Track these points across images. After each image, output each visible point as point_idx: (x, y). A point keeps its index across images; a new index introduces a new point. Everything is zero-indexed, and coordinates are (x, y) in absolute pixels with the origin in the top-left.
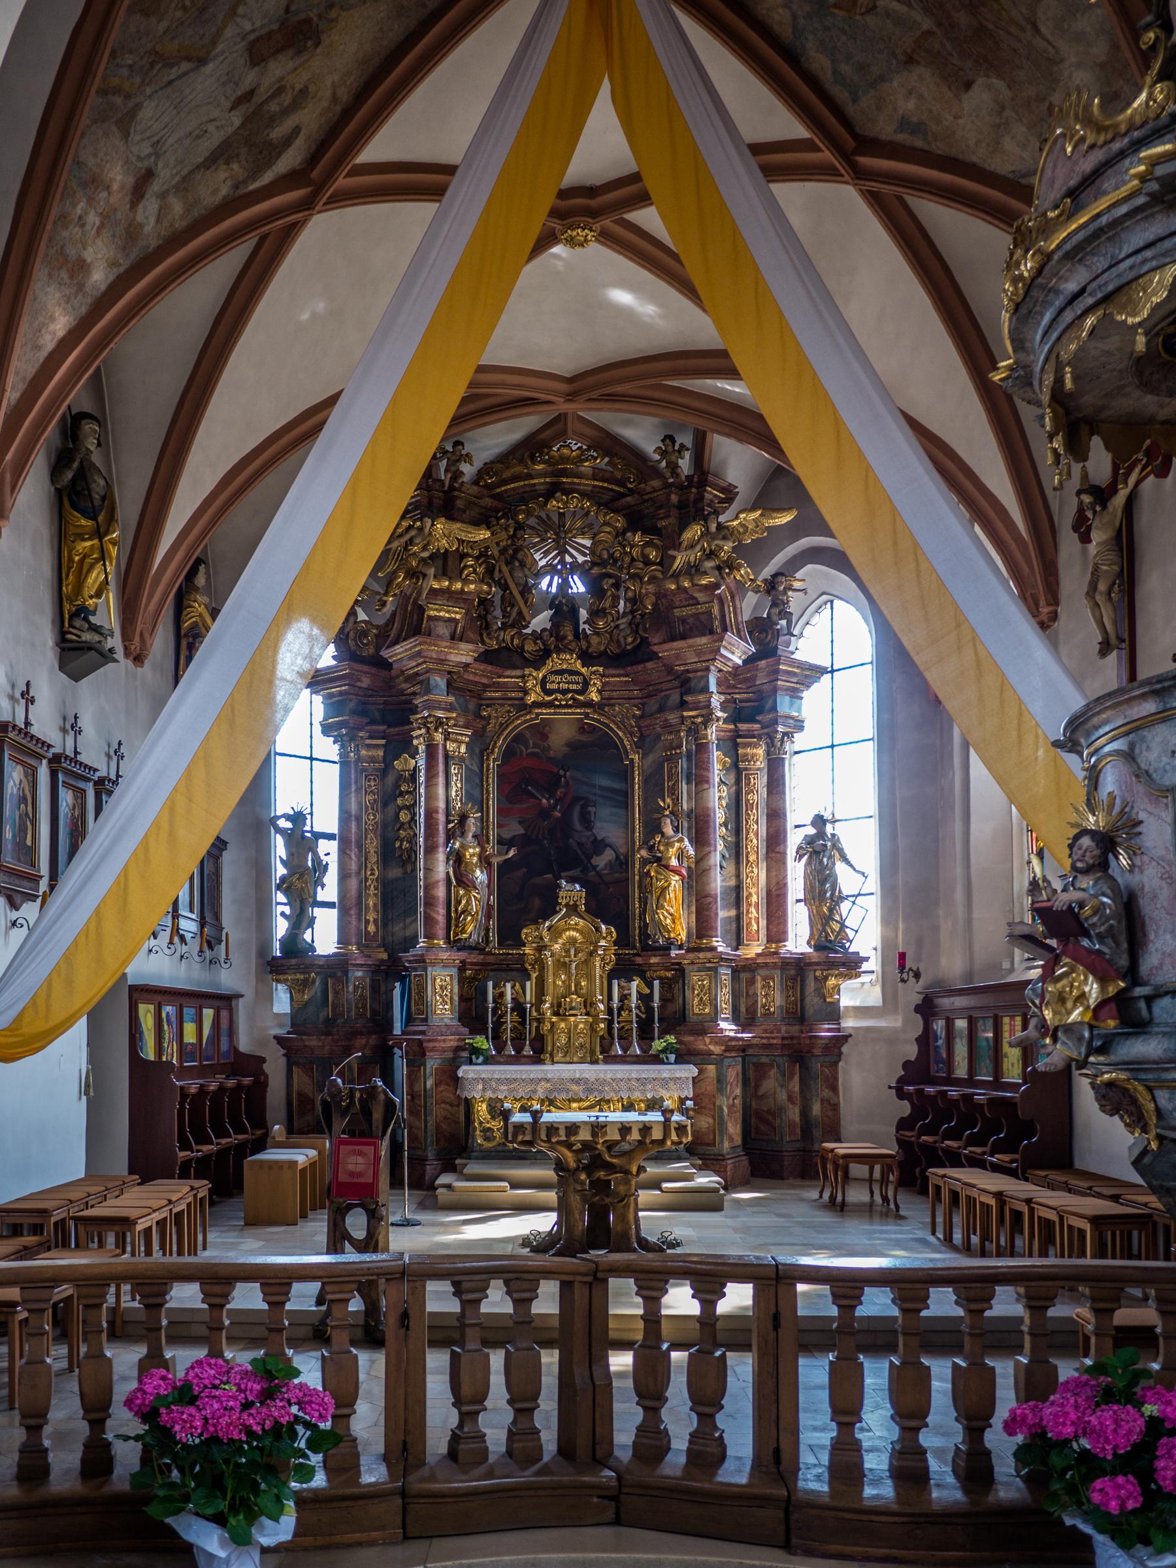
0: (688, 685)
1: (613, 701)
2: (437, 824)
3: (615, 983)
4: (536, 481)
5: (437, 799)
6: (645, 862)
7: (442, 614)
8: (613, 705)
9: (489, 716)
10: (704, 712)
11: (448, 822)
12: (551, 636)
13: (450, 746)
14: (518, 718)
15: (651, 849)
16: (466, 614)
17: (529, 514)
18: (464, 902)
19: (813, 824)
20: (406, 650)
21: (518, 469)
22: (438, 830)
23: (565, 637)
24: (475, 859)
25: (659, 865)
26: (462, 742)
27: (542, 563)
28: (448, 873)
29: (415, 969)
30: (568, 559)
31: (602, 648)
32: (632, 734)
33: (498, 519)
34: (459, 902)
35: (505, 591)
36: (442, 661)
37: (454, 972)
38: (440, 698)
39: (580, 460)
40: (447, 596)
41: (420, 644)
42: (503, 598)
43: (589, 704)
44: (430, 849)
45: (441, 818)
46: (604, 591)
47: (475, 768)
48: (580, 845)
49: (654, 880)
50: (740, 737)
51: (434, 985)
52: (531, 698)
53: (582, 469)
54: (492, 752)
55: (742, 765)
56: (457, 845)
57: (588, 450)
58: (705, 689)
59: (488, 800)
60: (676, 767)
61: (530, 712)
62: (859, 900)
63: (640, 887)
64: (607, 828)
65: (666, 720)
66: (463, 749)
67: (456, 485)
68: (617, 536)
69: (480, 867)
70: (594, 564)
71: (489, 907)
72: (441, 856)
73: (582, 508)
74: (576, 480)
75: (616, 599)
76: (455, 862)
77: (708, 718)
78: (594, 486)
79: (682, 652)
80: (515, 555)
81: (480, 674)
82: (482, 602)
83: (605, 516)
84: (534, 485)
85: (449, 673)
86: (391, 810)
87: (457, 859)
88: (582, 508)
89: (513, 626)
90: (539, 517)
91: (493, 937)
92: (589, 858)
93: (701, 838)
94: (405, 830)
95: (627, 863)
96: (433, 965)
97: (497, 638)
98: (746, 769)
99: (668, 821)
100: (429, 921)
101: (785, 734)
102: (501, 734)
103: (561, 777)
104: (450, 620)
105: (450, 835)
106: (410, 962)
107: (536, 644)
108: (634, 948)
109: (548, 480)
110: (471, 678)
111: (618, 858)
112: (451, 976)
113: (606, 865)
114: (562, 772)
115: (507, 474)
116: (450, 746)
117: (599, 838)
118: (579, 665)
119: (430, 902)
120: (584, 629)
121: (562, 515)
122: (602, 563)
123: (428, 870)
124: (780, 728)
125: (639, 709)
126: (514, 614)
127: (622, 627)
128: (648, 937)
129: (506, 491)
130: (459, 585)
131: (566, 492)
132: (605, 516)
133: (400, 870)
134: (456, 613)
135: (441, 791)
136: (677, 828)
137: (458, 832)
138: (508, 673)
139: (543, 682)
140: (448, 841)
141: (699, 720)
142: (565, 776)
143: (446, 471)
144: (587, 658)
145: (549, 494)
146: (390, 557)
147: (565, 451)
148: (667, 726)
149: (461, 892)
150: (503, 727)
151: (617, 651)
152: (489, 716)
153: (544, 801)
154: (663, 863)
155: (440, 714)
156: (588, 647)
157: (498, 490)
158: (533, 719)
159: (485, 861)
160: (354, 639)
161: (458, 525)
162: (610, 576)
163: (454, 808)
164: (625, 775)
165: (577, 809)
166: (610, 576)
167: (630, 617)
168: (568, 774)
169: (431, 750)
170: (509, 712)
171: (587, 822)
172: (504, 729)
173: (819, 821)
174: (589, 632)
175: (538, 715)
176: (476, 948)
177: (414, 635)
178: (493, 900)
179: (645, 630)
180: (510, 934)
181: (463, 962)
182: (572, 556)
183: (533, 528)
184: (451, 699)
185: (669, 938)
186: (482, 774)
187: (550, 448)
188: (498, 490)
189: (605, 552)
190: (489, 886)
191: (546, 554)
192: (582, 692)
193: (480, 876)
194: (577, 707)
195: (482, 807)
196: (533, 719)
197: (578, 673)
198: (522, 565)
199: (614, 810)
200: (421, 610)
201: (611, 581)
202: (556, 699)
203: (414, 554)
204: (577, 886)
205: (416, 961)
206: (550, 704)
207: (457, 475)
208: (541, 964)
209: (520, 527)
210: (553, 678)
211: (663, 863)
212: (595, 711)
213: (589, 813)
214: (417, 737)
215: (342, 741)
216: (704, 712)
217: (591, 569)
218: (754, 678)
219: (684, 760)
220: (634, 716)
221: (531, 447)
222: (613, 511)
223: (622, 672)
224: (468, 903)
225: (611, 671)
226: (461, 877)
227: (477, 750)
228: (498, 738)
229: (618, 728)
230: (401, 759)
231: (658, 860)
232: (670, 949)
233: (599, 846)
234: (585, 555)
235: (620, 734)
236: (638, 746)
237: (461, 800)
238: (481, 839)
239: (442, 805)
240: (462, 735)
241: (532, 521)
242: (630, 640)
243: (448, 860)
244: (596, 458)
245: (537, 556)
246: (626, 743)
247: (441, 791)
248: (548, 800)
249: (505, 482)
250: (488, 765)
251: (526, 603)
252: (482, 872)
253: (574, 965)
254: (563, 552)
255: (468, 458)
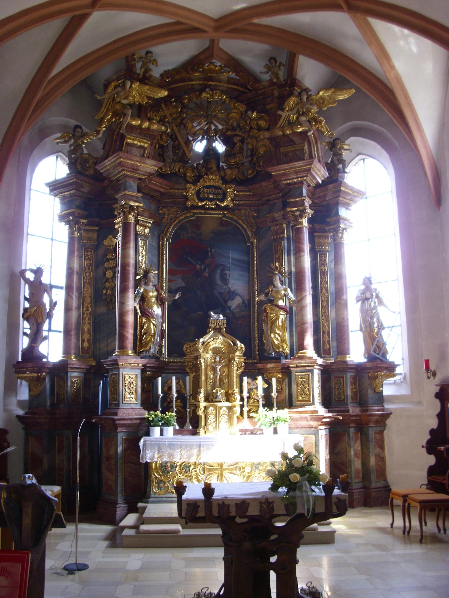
0: (292, 190)
1: (241, 207)
2: (129, 274)
3: (245, 379)
4: (194, 83)
5: (129, 257)
6: (261, 303)
7: (136, 142)
8: (240, 210)
9: (164, 213)
10: (301, 208)
11: (136, 274)
12: (203, 168)
13: (139, 229)
14: (182, 215)
15: (267, 295)
16: (151, 144)
17: (190, 100)
18: (146, 326)
19: (364, 284)
20: (112, 163)
21: (184, 74)
22: (129, 277)
23: (211, 168)
24: (154, 300)
25: (272, 305)
26: (145, 227)
27: (198, 128)
28: (135, 308)
29: (112, 370)
30: (213, 127)
31: (234, 177)
32: (251, 227)
33: (171, 103)
34: (142, 327)
35: (174, 142)
36: (135, 169)
37: (138, 372)
38: (133, 194)
39: (220, 71)
40: (139, 131)
41: (121, 158)
42: (174, 146)
43: (226, 208)
44: (124, 290)
45: (132, 270)
46: (235, 144)
47: (155, 244)
48: (220, 294)
49: (269, 315)
50: (315, 232)
51: (124, 381)
52: (189, 204)
53: (222, 77)
54: (166, 235)
55: (317, 249)
56: (142, 290)
57: (225, 66)
58: (301, 195)
59: (162, 264)
60: (281, 245)
61: (189, 212)
62: (394, 328)
63: (258, 321)
64: (237, 283)
65: (274, 217)
66: (147, 231)
67: (147, 75)
68: (242, 114)
69: (157, 305)
70: (228, 130)
71: (162, 331)
72: (131, 294)
73: (221, 99)
74: (218, 84)
75: (241, 149)
76: (140, 301)
77: (303, 213)
78: (228, 88)
79: (286, 171)
80: (182, 124)
81: (158, 185)
82: (161, 147)
83: (235, 104)
84: (193, 85)
85: (140, 179)
86: (101, 269)
87: (143, 299)
88: (221, 99)
89: (179, 161)
90: (195, 103)
91: (165, 351)
92: (226, 302)
93: (299, 288)
94: (109, 283)
95: (249, 306)
96: (124, 367)
97: (170, 167)
98: (320, 251)
99: (278, 277)
100: (122, 338)
101: (344, 229)
102: (171, 224)
103: (208, 252)
104: (141, 147)
105: (137, 283)
106: (108, 365)
107: (193, 172)
108: (255, 358)
109: (201, 83)
110: (153, 187)
111: (244, 302)
112: (137, 375)
113: (237, 306)
114: (209, 249)
115: (177, 77)
116: (139, 229)
117: (232, 289)
118: (219, 183)
119: (123, 324)
120: (222, 166)
121: (209, 103)
122: (234, 129)
123: (123, 304)
124: (342, 226)
125: (256, 212)
126: (180, 154)
127: (245, 164)
128: (265, 351)
129: (177, 87)
130: (146, 125)
131: (212, 90)
132: (235, 104)
133: (105, 308)
134: (145, 143)
135: (132, 252)
136: (282, 281)
137: (142, 283)
138: (177, 186)
139: (198, 193)
140: (136, 287)
141: (298, 213)
142: (211, 251)
143: (141, 68)
144: (225, 181)
145: (203, 89)
146: (104, 106)
147: (212, 67)
148: (274, 220)
149: (144, 320)
150: (172, 220)
151: (243, 178)
152: (164, 213)
153: (198, 266)
154: (275, 303)
155: (132, 203)
156: (225, 176)
157: (172, 86)
158: (190, 216)
159: (160, 301)
160: (81, 164)
161: (148, 87)
162: (238, 135)
163: (141, 267)
164: (248, 252)
165: (218, 271)
166: (238, 135)
167: (250, 159)
168: (213, 250)
169: (126, 226)
170: (176, 211)
171: (225, 280)
172: (173, 222)
173: (368, 282)
174: (225, 167)
175: (194, 214)
176: (154, 357)
177: (118, 151)
178: (165, 326)
179: (260, 166)
180: (176, 348)
181: (144, 365)
182: (215, 125)
183: (191, 109)
184: (140, 195)
185: (279, 352)
186: (160, 249)
187: (204, 65)
188: (172, 86)
189: (235, 122)
190: (162, 317)
191: (199, 124)
192: (222, 201)
193: (157, 310)
194: (218, 210)
195: (160, 268)
196: (190, 216)
197: (220, 188)
198: (185, 126)
199: (241, 273)
200: (123, 137)
201: (239, 138)
202: (206, 204)
203: (119, 102)
204: (221, 316)
205: (113, 365)
206: (203, 207)
207: (147, 70)
208: (196, 368)
209: (184, 106)
210: (204, 190)
211: (275, 303)
212: (229, 213)
213: (226, 274)
214: (118, 223)
215: (69, 224)
216: (301, 208)
217: (226, 132)
218: (325, 196)
219: (286, 241)
220: (253, 216)
221: (192, 64)
222: (238, 101)
223: (246, 188)
224: (149, 327)
225: (241, 188)
226: (144, 311)
227: (156, 234)
228: (170, 227)
229: (244, 223)
230: (108, 239)
231: (271, 302)
232: (280, 359)
233: (232, 294)
234: (222, 125)
235: (245, 227)
236: (256, 234)
237: (145, 263)
238: (158, 289)
239: (132, 261)
240: (147, 222)
241: (192, 106)
242: (250, 172)
243: (135, 298)
244: (230, 72)
245: (195, 124)
246: (249, 232)
247: (132, 252)
248: (200, 266)
249: (176, 82)
250: (163, 243)
251: (188, 148)
252: (158, 308)
253: (218, 369)
254: (209, 123)
255: (155, 62)
